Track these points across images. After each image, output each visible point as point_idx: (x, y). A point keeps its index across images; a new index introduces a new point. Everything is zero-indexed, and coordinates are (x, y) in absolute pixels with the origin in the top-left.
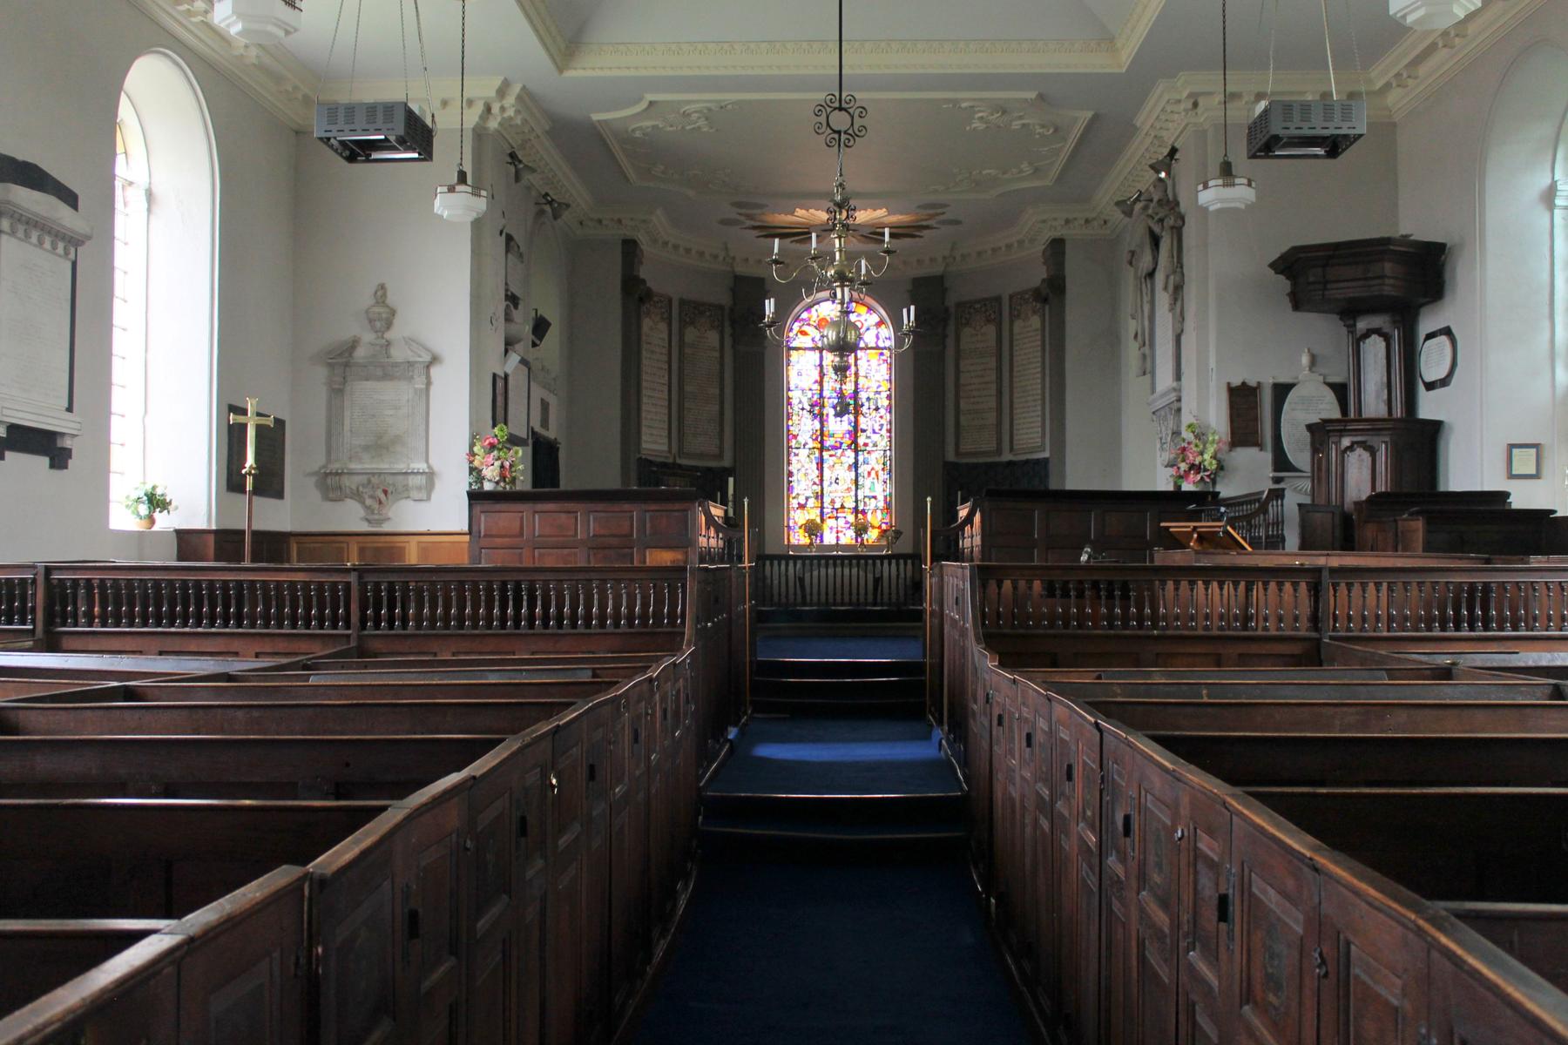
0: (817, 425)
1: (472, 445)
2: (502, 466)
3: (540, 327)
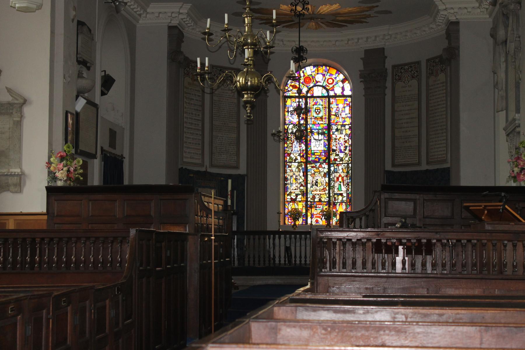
0: (303, 147)
1: (50, 157)
2: (68, 171)
3: (108, 82)
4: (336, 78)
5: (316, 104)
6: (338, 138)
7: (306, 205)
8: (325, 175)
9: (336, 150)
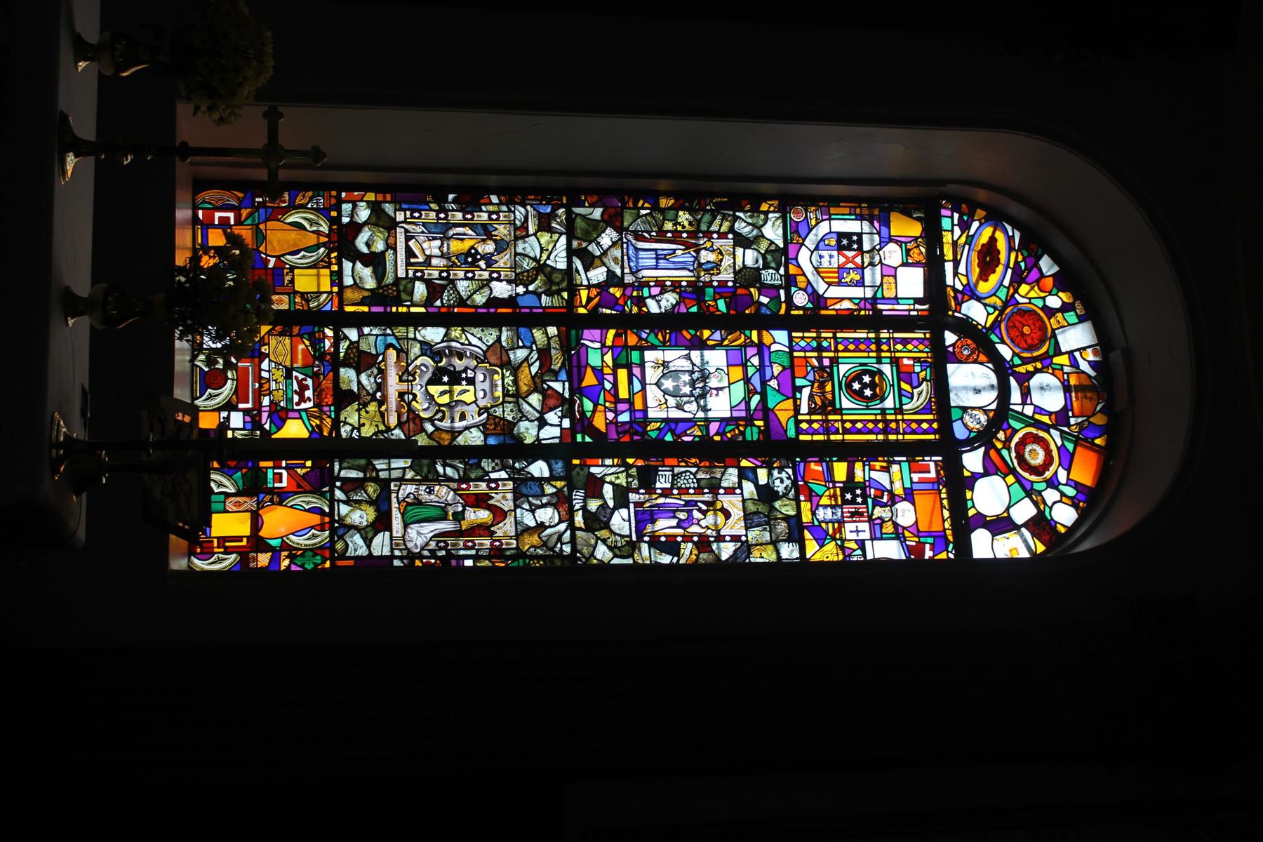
4: (1053, 483)
5: (904, 375)
6: (726, 501)
7: (319, 318)
8: (492, 425)
9: (650, 489)
